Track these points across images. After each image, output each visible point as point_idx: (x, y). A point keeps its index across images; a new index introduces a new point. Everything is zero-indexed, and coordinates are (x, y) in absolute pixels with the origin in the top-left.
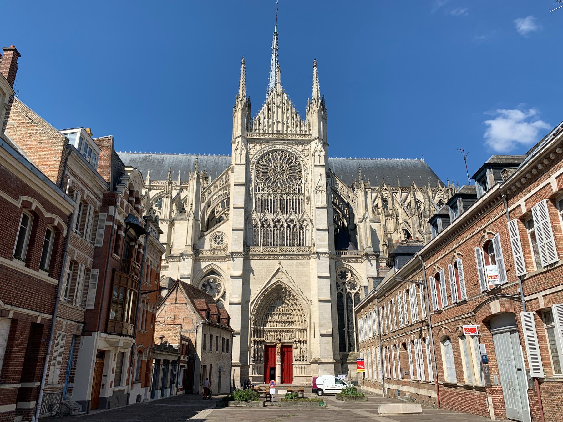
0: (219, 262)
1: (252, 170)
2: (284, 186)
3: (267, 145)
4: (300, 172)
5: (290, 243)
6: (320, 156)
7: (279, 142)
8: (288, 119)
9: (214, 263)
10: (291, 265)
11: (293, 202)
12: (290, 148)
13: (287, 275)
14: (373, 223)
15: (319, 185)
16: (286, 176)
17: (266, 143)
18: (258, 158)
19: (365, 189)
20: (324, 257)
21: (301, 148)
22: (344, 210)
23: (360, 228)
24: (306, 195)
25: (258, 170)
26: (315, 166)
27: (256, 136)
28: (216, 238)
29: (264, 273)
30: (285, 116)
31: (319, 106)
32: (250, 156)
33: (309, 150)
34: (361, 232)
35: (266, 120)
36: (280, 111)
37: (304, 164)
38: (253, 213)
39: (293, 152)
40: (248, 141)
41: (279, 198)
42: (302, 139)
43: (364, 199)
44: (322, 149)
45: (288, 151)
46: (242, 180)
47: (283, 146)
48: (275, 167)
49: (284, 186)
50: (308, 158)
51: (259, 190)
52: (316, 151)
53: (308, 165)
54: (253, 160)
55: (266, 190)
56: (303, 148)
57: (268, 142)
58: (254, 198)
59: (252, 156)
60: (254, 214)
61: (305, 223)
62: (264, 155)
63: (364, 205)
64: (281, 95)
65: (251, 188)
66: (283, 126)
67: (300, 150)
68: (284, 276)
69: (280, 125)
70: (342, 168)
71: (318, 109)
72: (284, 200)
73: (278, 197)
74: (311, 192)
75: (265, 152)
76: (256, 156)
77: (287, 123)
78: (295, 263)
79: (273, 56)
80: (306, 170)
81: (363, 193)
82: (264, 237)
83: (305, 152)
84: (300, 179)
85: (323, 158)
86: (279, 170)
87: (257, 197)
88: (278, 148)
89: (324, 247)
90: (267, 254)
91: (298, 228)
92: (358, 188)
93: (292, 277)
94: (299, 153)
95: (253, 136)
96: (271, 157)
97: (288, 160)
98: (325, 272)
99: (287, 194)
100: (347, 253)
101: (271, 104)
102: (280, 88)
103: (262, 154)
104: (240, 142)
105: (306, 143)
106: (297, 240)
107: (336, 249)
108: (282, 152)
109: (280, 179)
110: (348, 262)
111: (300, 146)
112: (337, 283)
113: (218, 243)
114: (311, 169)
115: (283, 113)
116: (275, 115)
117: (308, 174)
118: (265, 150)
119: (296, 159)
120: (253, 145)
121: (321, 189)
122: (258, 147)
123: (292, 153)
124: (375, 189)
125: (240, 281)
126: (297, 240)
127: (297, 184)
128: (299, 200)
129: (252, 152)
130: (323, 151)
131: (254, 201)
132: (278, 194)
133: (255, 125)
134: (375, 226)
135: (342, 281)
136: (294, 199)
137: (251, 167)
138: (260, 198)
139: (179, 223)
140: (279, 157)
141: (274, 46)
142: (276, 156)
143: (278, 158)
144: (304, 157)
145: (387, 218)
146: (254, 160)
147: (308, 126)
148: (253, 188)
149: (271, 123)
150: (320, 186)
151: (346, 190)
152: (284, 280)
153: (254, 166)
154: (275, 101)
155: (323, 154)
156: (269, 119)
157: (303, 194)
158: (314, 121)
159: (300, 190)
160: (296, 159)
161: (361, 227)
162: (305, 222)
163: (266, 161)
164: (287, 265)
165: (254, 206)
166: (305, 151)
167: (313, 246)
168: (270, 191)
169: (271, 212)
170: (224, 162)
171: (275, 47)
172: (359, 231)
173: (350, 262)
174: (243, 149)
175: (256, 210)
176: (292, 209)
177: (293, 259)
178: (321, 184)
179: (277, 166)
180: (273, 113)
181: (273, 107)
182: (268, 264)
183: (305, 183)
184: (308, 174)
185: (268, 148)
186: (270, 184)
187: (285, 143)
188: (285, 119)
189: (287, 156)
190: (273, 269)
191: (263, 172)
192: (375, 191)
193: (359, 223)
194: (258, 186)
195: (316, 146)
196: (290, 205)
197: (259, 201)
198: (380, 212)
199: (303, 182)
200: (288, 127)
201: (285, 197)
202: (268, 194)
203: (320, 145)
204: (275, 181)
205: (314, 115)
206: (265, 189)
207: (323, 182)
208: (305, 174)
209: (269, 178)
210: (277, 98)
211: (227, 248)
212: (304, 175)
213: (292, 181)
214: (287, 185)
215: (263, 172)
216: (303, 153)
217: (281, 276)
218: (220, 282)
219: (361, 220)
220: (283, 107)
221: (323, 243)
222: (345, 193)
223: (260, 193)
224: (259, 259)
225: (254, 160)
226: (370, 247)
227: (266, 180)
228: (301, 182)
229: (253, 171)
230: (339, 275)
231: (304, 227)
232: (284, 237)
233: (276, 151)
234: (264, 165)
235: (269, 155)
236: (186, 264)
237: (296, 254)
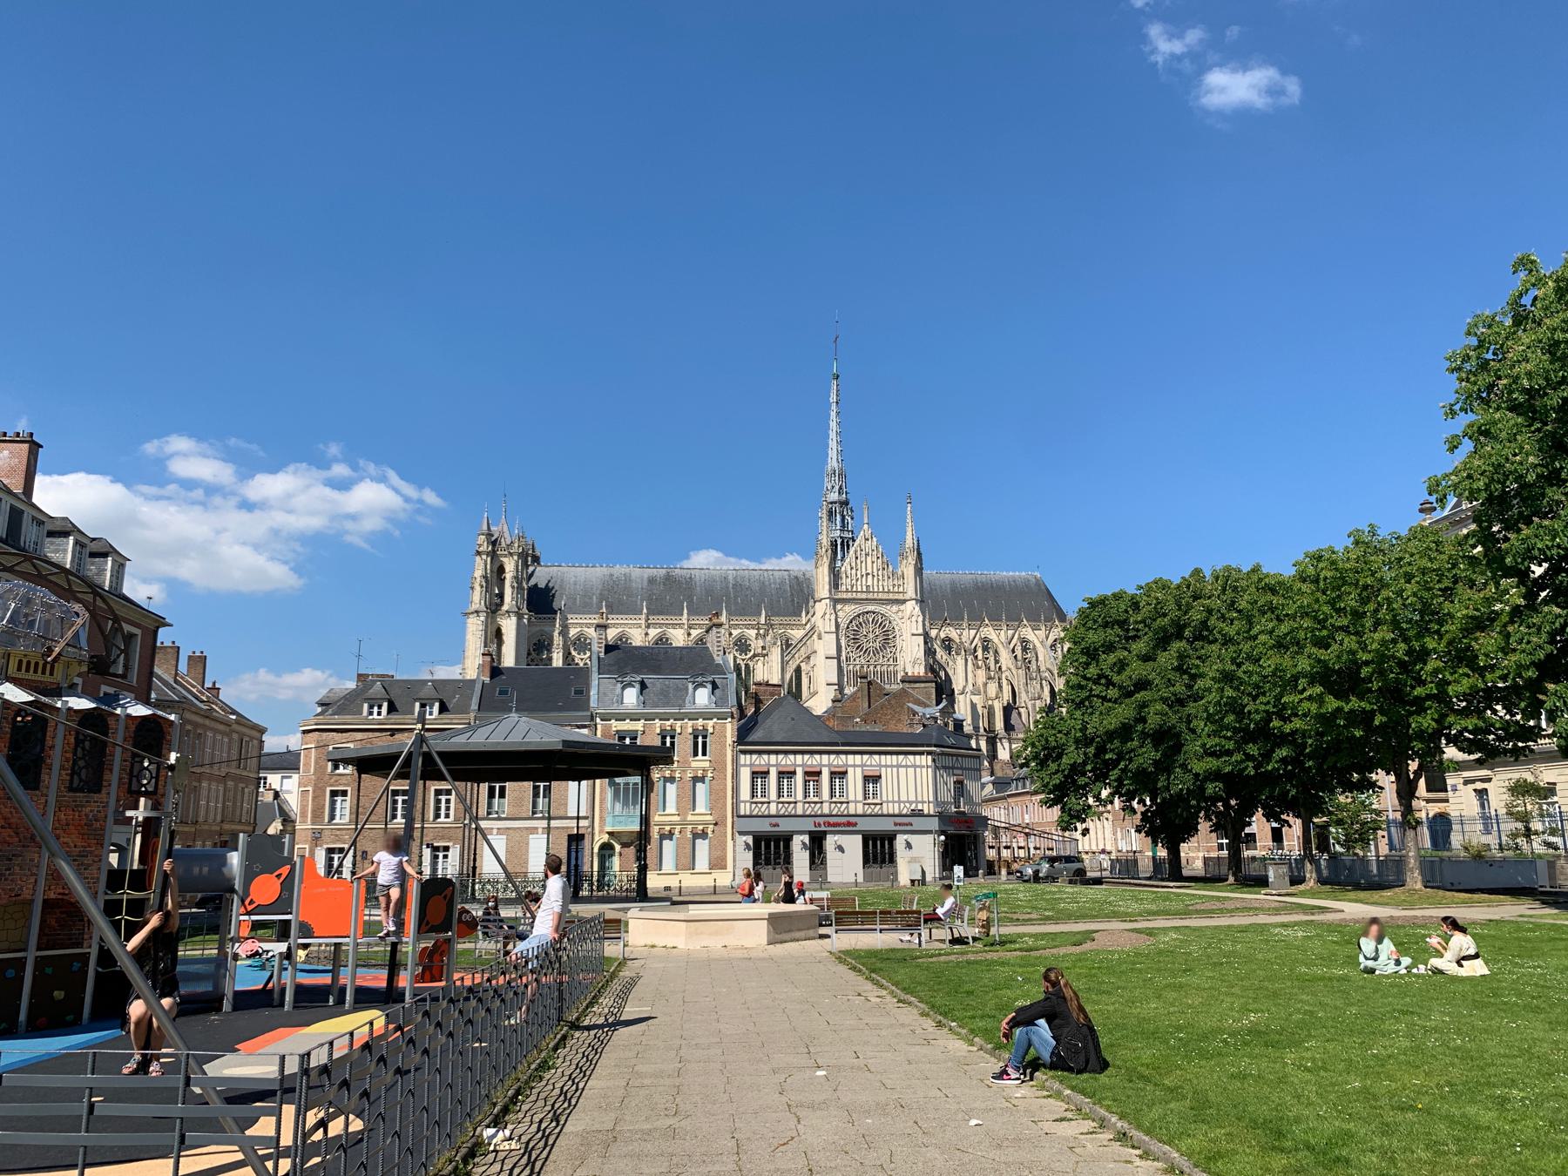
17: (856, 604)
21: (895, 608)
26: (913, 635)
32: (839, 620)
35: (854, 571)
36: (869, 559)
40: (836, 601)
46: (833, 652)
69: (870, 577)
73: (872, 668)
79: (833, 414)
85: (920, 624)
86: (871, 636)
92: (958, 654)
95: (840, 596)
114: (907, 636)
115: (873, 562)
122: (848, 608)
129: (840, 614)
134: (976, 699)
140: (871, 620)
141: (833, 398)
146: (843, 626)
149: (859, 576)
154: (863, 547)
155: (921, 619)
159: (895, 660)
188: (875, 570)
195: (912, 608)
203: (917, 608)
225: (843, 626)
233: (867, 613)
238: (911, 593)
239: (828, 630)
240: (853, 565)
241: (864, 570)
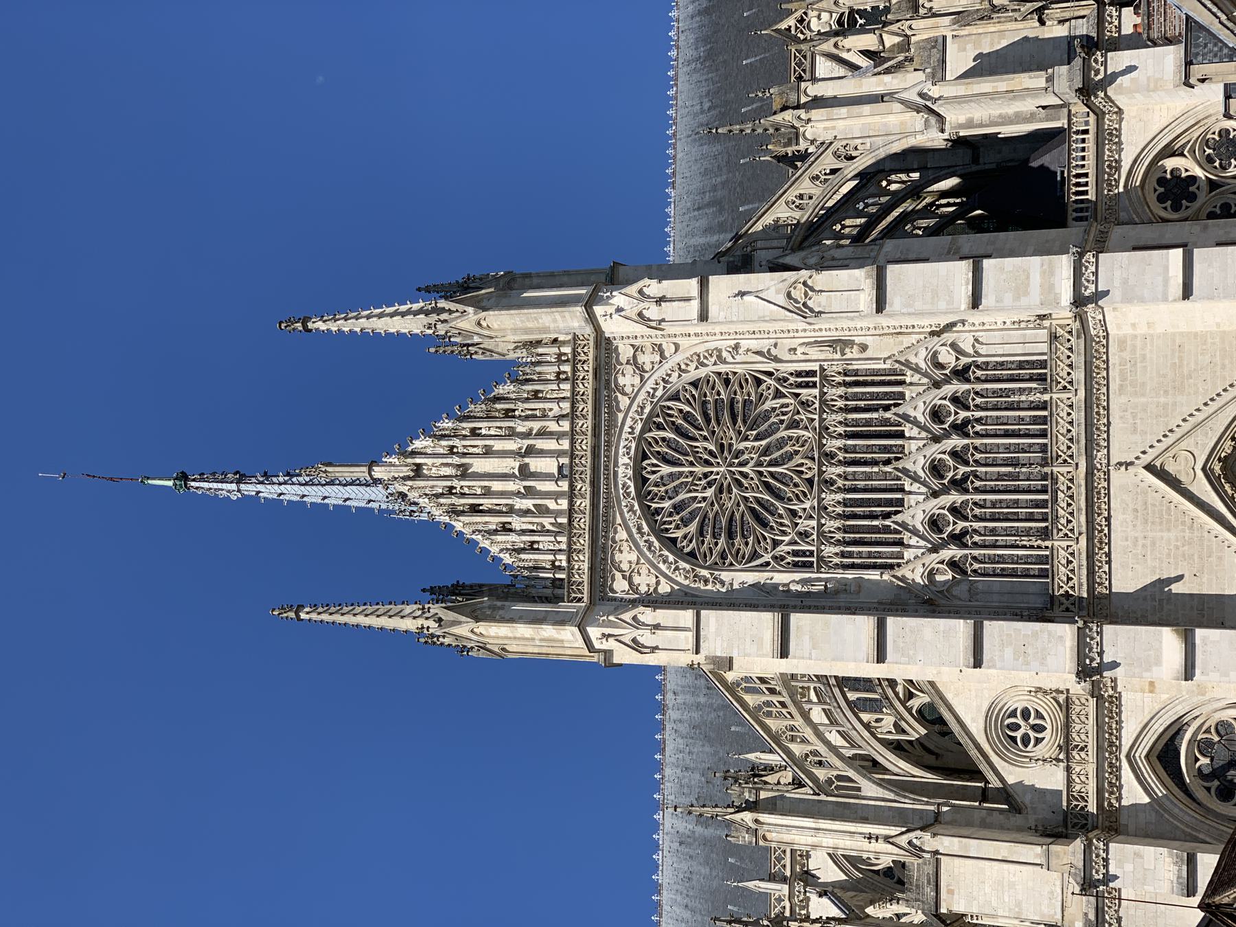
0: (1119, 730)
1: (722, 583)
2: (788, 448)
3: (619, 520)
4: (727, 382)
5: (1035, 420)
6: (660, 300)
7: (607, 468)
8: (512, 434)
9: (1125, 750)
10: (1134, 416)
11: (857, 410)
12: (630, 423)
13: (1179, 432)
14: (944, 70)
15: (781, 300)
16: (746, 439)
17: (609, 523)
18: (671, 558)
19: (798, 107)
20: (1096, 274)
21: (628, 379)
22: (888, 193)
23: (970, 124)
24: (827, 354)
25: (723, 556)
26: (704, 316)
27: (583, 563)
28: (1014, 739)
29: (1172, 535)
30: (498, 445)
31: (461, 307)
32: (664, 588)
33: (637, 343)
34: (986, 119)
35: (517, 523)
36: (480, 465)
37: (693, 366)
38: (903, 579)
39: (647, 410)
41: (840, 470)
42: (590, 376)
43: (843, 111)
44: (633, 289)
45: (643, 431)
46: (766, 622)
47: (621, 451)
48: (710, 484)
49: (788, 448)
50: (669, 349)
51: (804, 554)
52: (640, 315)
53: (700, 349)
54: (681, 579)
55: (805, 524)
56: (629, 369)
57: (606, 515)
58: (840, 575)
59: (662, 580)
60: (909, 575)
61: (947, 357)
62: (659, 532)
63: (866, 109)
64: (418, 461)
65: (799, 588)
66: (542, 453)
67: (637, 380)
68: (1183, 445)
69: (536, 464)
70: (709, 205)
71: (470, 310)
72: (846, 450)
73: (833, 471)
74: (811, 336)
75: (646, 528)
76: (663, 567)
77: (527, 435)
78: (1123, 399)
79: (268, 491)
80: (719, 357)
81: (815, 114)
82: (1008, 532)
83: (645, 359)
84: (759, 382)
87: (837, 560)
88: (630, 472)
89: (1050, 273)
90: (1083, 519)
91: (967, 387)
92: (795, 136)
93: (1186, 411)
94: (649, 386)
96: (667, 504)
97: (678, 430)
98: (1166, 268)
99: (821, 436)
100: (1078, 176)
101: (454, 500)
102: (391, 465)
103: (653, 539)
104: (608, 631)
105: (609, 357)
106: (1022, 391)
107: (1062, 224)
108: (645, 457)
109: (759, 464)
110: (1118, 169)
111: (621, 381)
112: (1211, 216)
113: (1039, 729)
114: (714, 337)
115: (488, 452)
116: (497, 486)
117: (736, 347)
118: (639, 529)
119: (675, 397)
120: (618, 575)
121: (798, 294)
122: (626, 557)
123: (650, 415)
124: (799, 64)
125: (1204, 639)
126: (1022, 391)
127: (778, 394)
128: (846, 384)
129: (644, 581)
130: (640, 284)
131: (850, 575)
132: (821, 473)
133: (536, 568)
134: (959, 59)
135: (1202, 197)
136: (841, 403)
137: (709, 587)
138: (837, 549)
139: (951, 892)
140: (666, 469)
141: (228, 489)
142: (662, 482)
143: (671, 475)
144: (667, 366)
145: (922, 11)
147: (540, 350)
148: (798, 576)
149: (528, 504)
150: (789, 295)
151: (805, 186)
152: (1202, 444)
153: (705, 573)
155: (654, 287)
156: (511, 510)
157: (822, 369)
158: (520, 325)
159: (805, 378)
160: (675, 397)
161: (962, 119)
162: (941, 359)
163: (685, 522)
164: (1135, 431)
165: (873, 575)
166: (641, 359)
167: (1046, 323)
168: (807, 505)
169: (900, 502)
170: (689, 699)
171: (234, 486)
172: (981, 125)
173: (1118, 162)
174: (635, 618)
175: (891, 567)
176: (888, 415)
177: (1107, 409)
178: (778, 292)
179: (706, 475)
180: (488, 493)
181: (463, 495)
182: (1129, 517)
183: (777, 360)
184: (736, 347)
185: (628, 514)
186: (780, 507)
187: (608, 444)
188: (511, 445)
189: (662, 434)
190: (1151, 494)
191: (731, 536)
192: (807, 64)
193: (947, 127)
194: (790, 559)
196: (868, 423)
197: (850, 555)
198: (897, 39)
199: (770, 367)
200: (542, 434)
201: (833, 444)
202: (820, 517)
203: (619, 299)
204: (767, 486)
205: (495, 326)
206: (800, 528)
207: (770, 283)
208: (739, 358)
209: (752, 510)
210: (428, 478)
211: (1058, 691)
212: (739, 366)
213: (766, 415)
214: (783, 434)
215: (731, 536)
216: (647, 367)
217: (1181, 459)
218: (1212, 723)
219: (933, 120)
220: (464, 455)
221: (1036, 279)
222: (816, 190)
223: (820, 551)
224: (1108, 555)
225: (680, 575)
226: (1050, 79)
227: (764, 524)
228: (770, 374)
229: (725, 576)
230: (1176, 208)
231: (964, 360)
232: (1008, 448)
233: (641, 481)
234: (701, 532)
235: (657, 511)
236: (1129, 867)
237: (1082, 393)
238: (570, 321)
239: (687, 639)
240: (494, 521)
241: (511, 486)
